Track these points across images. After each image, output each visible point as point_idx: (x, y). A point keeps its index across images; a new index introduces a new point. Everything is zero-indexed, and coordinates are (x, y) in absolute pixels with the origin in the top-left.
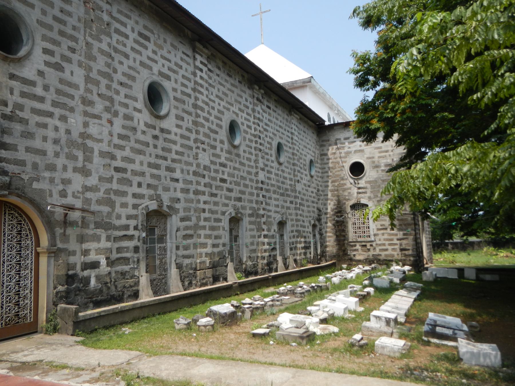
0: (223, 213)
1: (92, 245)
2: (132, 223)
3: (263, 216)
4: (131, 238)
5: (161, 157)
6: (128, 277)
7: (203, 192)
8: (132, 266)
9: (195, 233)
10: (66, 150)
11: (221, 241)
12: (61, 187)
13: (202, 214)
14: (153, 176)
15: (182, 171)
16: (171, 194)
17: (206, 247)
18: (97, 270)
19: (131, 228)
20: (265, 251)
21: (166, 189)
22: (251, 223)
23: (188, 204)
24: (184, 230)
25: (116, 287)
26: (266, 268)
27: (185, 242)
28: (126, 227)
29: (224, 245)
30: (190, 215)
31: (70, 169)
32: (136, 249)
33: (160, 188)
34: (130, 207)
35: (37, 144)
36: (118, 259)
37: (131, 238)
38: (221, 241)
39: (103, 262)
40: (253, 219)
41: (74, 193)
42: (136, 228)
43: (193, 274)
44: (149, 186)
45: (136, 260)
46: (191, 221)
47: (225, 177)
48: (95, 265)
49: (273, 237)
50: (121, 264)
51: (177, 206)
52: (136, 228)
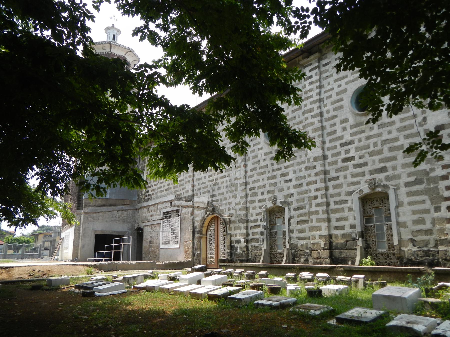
0: (351, 193)
1: (238, 232)
2: (259, 217)
4: (259, 226)
5: (277, 169)
7: (314, 181)
8: (260, 243)
9: (309, 218)
10: (230, 189)
11: (347, 224)
12: (228, 207)
13: (313, 201)
14: (271, 185)
15: (294, 172)
16: (286, 192)
17: (320, 230)
18: (240, 244)
19: (259, 220)
21: (281, 190)
22: (409, 194)
23: (301, 196)
24: (298, 217)
25: (252, 255)
27: (299, 227)
28: (256, 221)
30: (304, 204)
31: (231, 197)
32: (262, 233)
33: (276, 191)
34: (258, 208)
35: (221, 191)
36: (253, 239)
37: (259, 226)
38: (347, 224)
39: (243, 240)
41: (233, 207)
42: (261, 220)
43: (310, 253)
44: (268, 192)
45: (262, 239)
46: (305, 209)
47: (352, 154)
48: (239, 242)
51: (290, 200)
52: (261, 220)
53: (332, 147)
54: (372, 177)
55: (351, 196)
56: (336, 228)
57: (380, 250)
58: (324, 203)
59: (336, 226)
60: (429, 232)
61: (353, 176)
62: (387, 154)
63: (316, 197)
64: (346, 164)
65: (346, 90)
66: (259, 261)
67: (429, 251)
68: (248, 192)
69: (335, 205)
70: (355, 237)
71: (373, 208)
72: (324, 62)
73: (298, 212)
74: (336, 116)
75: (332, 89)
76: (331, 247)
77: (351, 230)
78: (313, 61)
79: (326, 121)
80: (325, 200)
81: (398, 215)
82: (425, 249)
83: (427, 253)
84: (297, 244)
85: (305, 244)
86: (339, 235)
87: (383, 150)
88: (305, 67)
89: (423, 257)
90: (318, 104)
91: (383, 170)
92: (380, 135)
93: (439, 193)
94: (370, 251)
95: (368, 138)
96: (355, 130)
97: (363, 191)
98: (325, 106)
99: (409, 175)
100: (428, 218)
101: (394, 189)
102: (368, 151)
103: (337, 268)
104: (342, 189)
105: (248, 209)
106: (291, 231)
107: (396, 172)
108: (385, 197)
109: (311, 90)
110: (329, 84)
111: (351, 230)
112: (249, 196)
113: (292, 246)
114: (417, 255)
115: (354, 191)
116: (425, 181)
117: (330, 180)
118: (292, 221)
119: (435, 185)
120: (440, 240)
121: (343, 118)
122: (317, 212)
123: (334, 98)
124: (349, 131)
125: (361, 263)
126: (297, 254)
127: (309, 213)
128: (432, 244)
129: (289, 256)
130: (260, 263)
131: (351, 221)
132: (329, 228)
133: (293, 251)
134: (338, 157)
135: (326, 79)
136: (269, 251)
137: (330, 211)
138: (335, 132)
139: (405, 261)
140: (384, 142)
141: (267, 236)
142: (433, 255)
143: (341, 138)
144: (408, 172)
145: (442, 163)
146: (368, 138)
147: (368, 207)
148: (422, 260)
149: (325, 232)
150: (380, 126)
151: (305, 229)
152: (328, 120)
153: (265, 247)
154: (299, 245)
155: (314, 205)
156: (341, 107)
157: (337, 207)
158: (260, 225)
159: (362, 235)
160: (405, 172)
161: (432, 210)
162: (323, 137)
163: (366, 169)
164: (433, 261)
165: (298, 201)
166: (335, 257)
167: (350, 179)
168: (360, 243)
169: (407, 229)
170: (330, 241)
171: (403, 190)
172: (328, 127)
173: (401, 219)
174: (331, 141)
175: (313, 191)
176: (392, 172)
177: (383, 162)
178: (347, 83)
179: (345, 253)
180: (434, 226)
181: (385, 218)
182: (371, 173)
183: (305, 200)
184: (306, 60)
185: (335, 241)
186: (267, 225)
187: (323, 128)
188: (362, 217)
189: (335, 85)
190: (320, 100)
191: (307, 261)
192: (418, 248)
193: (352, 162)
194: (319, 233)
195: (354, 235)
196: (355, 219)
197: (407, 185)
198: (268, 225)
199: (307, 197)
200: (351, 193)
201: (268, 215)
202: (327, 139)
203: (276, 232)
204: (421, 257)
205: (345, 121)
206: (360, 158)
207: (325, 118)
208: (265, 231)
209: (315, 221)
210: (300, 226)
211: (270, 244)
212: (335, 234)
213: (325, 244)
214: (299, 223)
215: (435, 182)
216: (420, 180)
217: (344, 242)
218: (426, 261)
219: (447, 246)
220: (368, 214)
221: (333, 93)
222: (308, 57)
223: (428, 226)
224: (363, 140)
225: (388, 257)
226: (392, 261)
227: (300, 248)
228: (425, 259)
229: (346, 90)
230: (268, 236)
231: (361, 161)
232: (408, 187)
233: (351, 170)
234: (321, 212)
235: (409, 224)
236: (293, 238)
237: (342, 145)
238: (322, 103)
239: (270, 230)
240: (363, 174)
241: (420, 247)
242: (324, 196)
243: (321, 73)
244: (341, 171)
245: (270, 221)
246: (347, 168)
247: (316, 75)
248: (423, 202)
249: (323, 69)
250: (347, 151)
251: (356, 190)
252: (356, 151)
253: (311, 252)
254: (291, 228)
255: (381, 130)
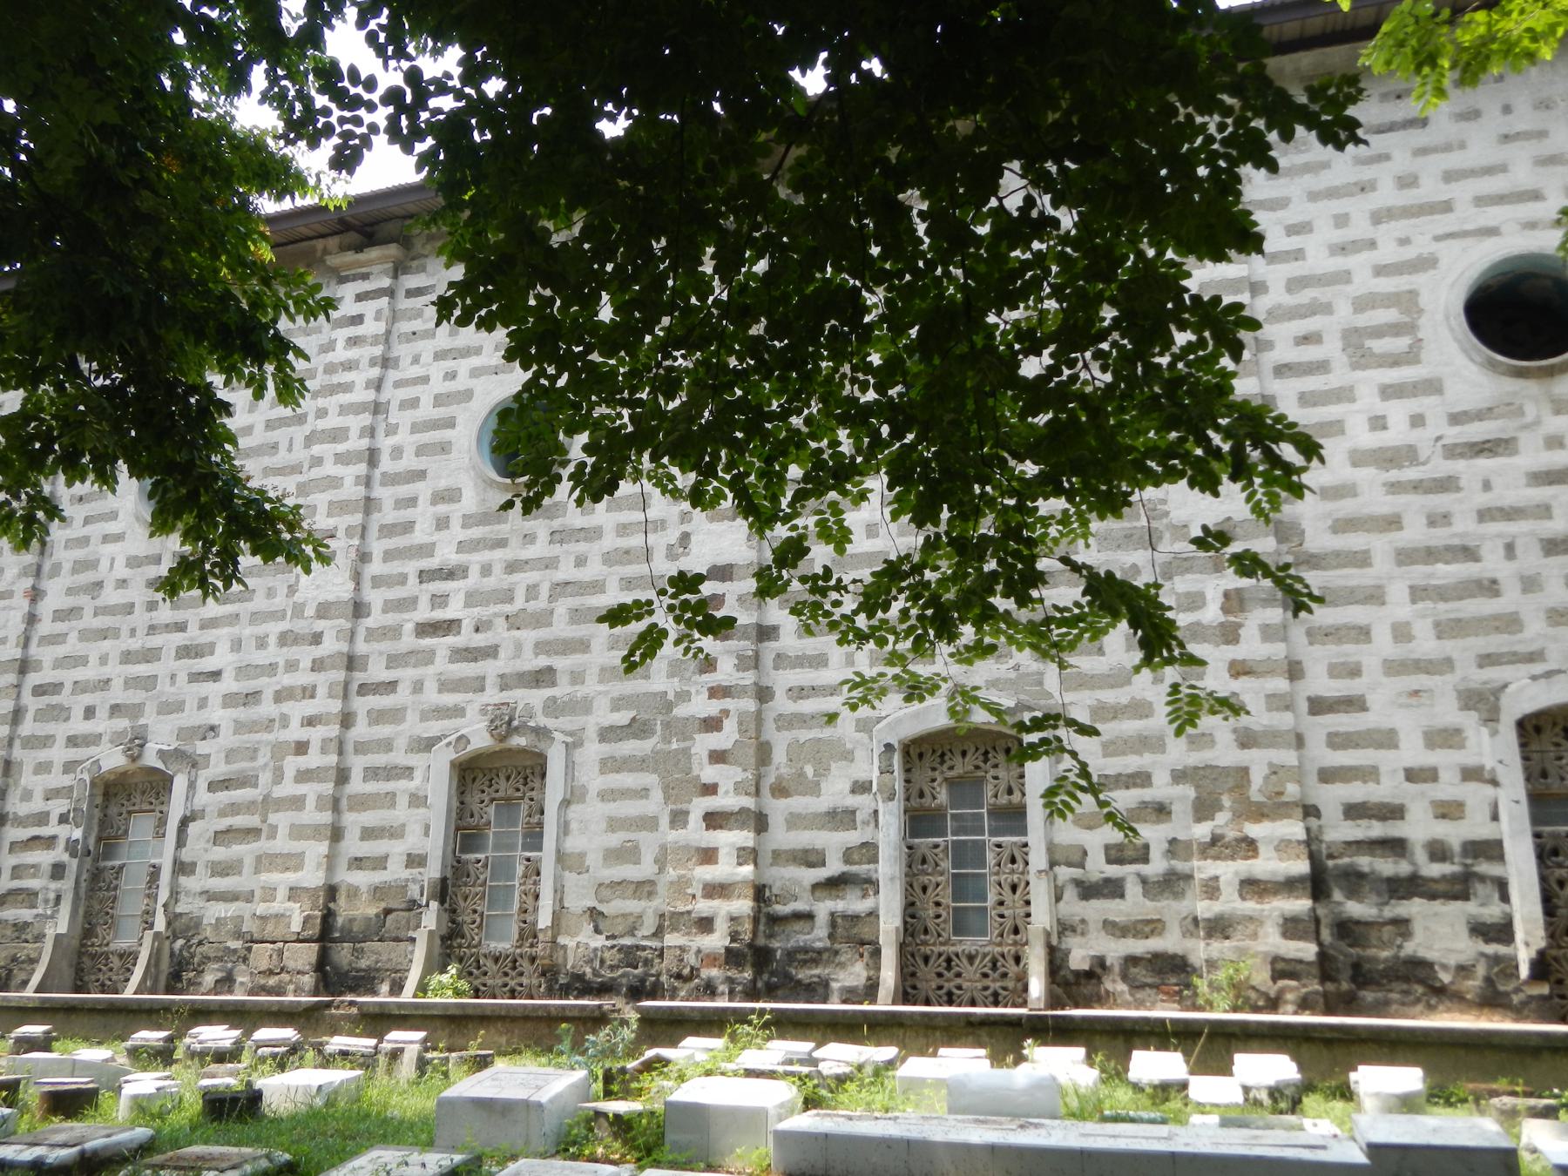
0: (427, 745)
2: (59, 806)
3: (712, 724)
4: (50, 841)
5: (167, 626)
6: (29, 937)
7: (304, 689)
8: (40, 911)
9: (264, 821)
11: (397, 849)
14: (131, 683)
15: (237, 645)
16: (191, 717)
17: (299, 867)
19: (54, 818)
20: (716, 890)
21: (171, 707)
22: (610, 765)
23: (246, 737)
24: (222, 813)
26: (714, 972)
27: (220, 853)
28: (42, 818)
29: (415, 860)
30: (253, 769)
32: (58, 871)
33: (150, 709)
37: (50, 841)
38: (397, 849)
40: (630, 747)
42: (63, 819)
44: (116, 710)
45: (52, 896)
46: (255, 786)
49: (841, 818)
50: (15, 905)
51: (202, 748)
52: (63, 819)
53: (390, 576)
54: (507, 696)
55: (426, 755)
56: (358, 863)
57: (493, 945)
58: (327, 769)
59: (359, 855)
60: (644, 888)
61: (445, 686)
62: (561, 628)
63: (301, 748)
64: (428, 642)
65: (467, 395)
66: (25, 983)
67: (638, 948)
68: (27, 699)
69: (365, 780)
70: (416, 896)
71: (493, 800)
72: (412, 281)
73: (224, 797)
74: (421, 475)
75: (425, 380)
76: (326, 932)
77: (406, 874)
78: (375, 269)
79: (383, 484)
80: (333, 759)
81: (564, 829)
82: (627, 941)
83: (630, 956)
84: (200, 918)
85: (232, 918)
86: (364, 889)
87: (552, 612)
88: (343, 280)
89: (618, 967)
90: (366, 419)
91: (542, 677)
92: (550, 564)
93: (688, 771)
94: (460, 946)
95: (512, 567)
96: (477, 532)
97: (468, 742)
98: (392, 430)
99: (617, 704)
100: (649, 844)
101: (567, 745)
102: (508, 608)
103: (338, 1007)
104: (400, 728)
105: (14, 770)
106: (182, 868)
107: (581, 691)
108: (532, 769)
109: (349, 366)
110: (416, 360)
111: (406, 874)
112: (29, 716)
113: (177, 924)
114: (602, 962)
115: (439, 739)
116: (659, 727)
117: (364, 689)
118: (193, 828)
119: (683, 745)
120: (673, 914)
121: (443, 484)
122: (297, 803)
123: (427, 411)
124: (457, 532)
125: (422, 988)
126: (193, 956)
127: (268, 804)
128: (648, 927)
129: (157, 965)
130: (29, 993)
131: (413, 841)
132: (331, 860)
133: (180, 942)
134: (406, 616)
135: (408, 341)
136: (75, 943)
137: (344, 803)
138: (408, 527)
139: (563, 980)
140: (562, 588)
141: (77, 882)
142: (647, 962)
143: (427, 550)
144: (616, 694)
145: (710, 679)
146: (512, 567)
147: (478, 796)
148: (613, 979)
149: (312, 877)
150: (557, 537)
151: (240, 861)
152: (391, 480)
153: (63, 928)
154: (205, 921)
155: (290, 773)
156: (444, 448)
157: (372, 787)
158: (54, 838)
159: (443, 891)
160: (606, 693)
161: (665, 821)
162: (363, 537)
163: (490, 669)
164: (643, 981)
165: (230, 755)
166: (336, 968)
167: (432, 696)
168: (431, 918)
169: (585, 876)
170: (329, 909)
171: (593, 750)
172: (388, 505)
173: (573, 844)
174: (389, 556)
175: (295, 722)
176: (569, 689)
177: (548, 653)
178: (476, 373)
179: (375, 954)
180: (661, 870)
181: (525, 836)
182: (505, 683)
183: (261, 754)
184: (350, 257)
185: (345, 911)
186: (85, 838)
187: (369, 505)
188: (453, 827)
189: (437, 370)
190: (377, 408)
191: (227, 982)
192: (608, 938)
193: (450, 640)
194: (291, 877)
195: (414, 891)
196: (427, 834)
197: (607, 734)
198: (92, 841)
199: (269, 743)
200: (427, 745)
201: (99, 800)
202: (377, 547)
203: (121, 867)
204: (612, 968)
205: (449, 496)
206: (477, 630)
207: (384, 474)
208: (75, 862)
209: (282, 831)
210: (222, 849)
211: (88, 914)
212: (350, 885)
213: (307, 920)
214: (221, 837)
215: (686, 737)
216: (645, 723)
217: (377, 915)
218: (624, 981)
219: (688, 934)
220: (473, 822)
221: (425, 394)
222: (359, 249)
223: (645, 869)
224: (498, 569)
225: (514, 968)
226: (525, 981)
227: (208, 933)
228: (623, 976)
229: (467, 395)
230: (83, 885)
231: (480, 640)
232: (609, 741)
233: (441, 664)
234: (311, 803)
235: (593, 860)
236: (187, 893)
237: (424, 576)
238: (381, 417)
239: (96, 860)
240: (479, 685)
241: (613, 937)
242: (334, 746)
243: (395, 316)
244: (406, 665)
245: (104, 823)
246: (428, 657)
247: (377, 318)
248: (644, 793)
249: (404, 304)
250: (439, 600)
251: (446, 736)
252: (467, 605)
253: (249, 949)
254: (186, 855)
255: (557, 550)
